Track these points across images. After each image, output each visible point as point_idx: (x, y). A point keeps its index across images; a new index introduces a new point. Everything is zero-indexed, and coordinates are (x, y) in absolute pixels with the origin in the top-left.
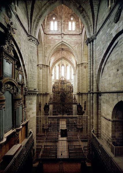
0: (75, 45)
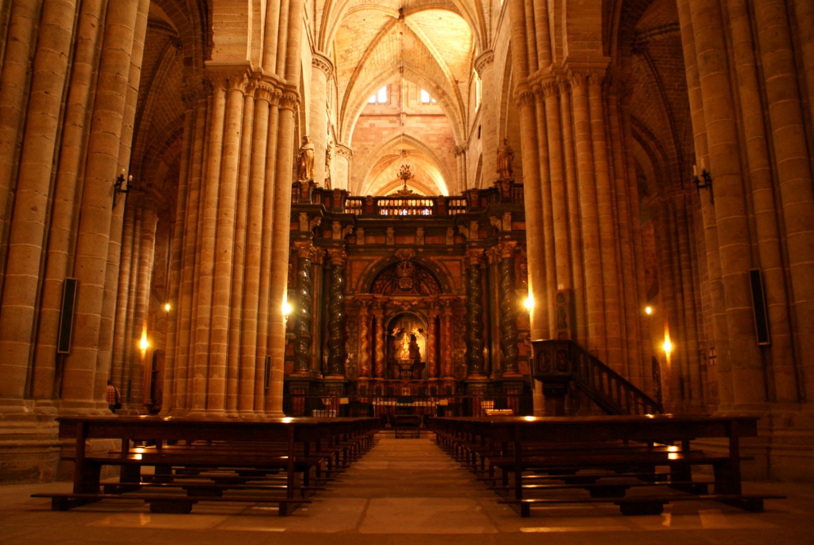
0: (443, 145)
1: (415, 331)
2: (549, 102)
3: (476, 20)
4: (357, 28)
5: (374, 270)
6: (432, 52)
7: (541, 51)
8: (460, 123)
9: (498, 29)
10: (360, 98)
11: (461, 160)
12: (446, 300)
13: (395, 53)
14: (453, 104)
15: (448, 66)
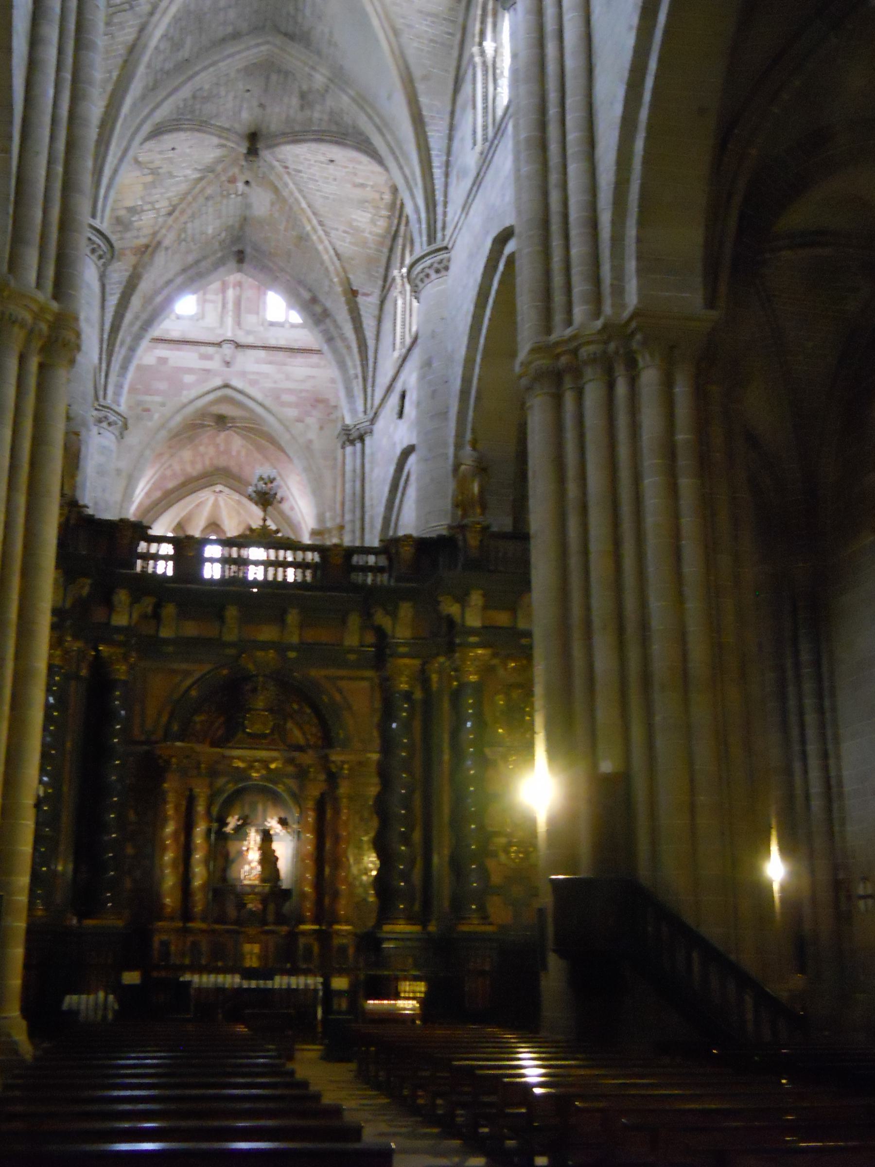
1: (273, 824)
2: (593, 394)
3: (415, 179)
4: (157, 163)
5: (194, 693)
6: (309, 228)
7: (579, 287)
8: (356, 377)
9: (466, 206)
10: (150, 308)
11: (354, 453)
12: (343, 762)
13: (230, 223)
14: (344, 339)
15: (339, 259)
